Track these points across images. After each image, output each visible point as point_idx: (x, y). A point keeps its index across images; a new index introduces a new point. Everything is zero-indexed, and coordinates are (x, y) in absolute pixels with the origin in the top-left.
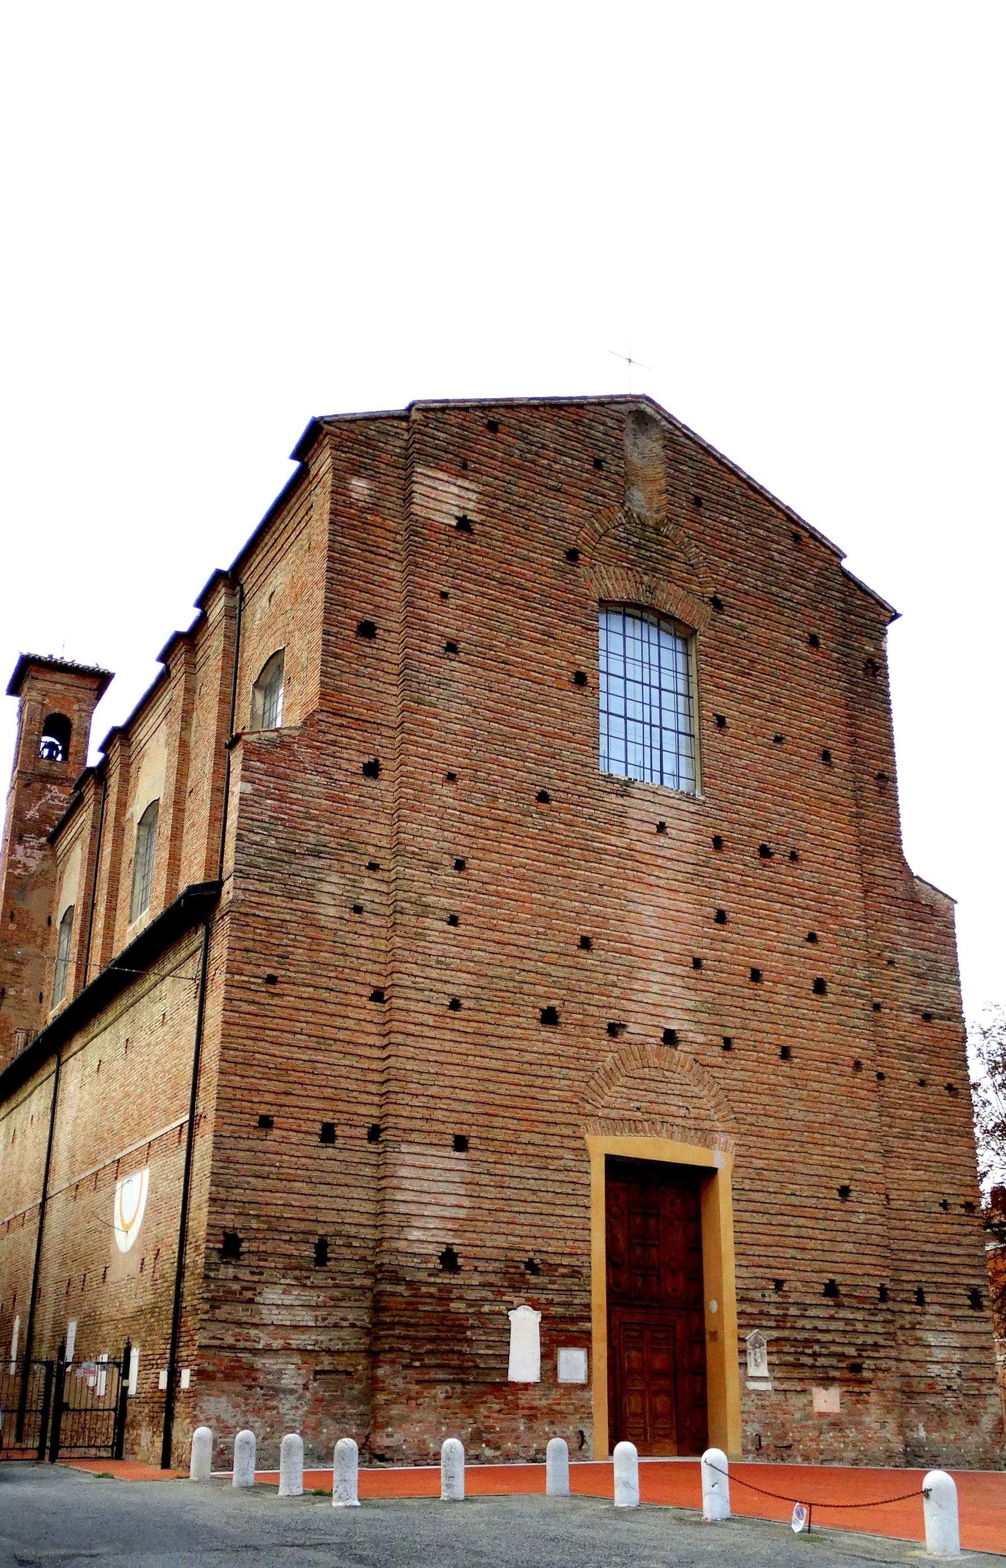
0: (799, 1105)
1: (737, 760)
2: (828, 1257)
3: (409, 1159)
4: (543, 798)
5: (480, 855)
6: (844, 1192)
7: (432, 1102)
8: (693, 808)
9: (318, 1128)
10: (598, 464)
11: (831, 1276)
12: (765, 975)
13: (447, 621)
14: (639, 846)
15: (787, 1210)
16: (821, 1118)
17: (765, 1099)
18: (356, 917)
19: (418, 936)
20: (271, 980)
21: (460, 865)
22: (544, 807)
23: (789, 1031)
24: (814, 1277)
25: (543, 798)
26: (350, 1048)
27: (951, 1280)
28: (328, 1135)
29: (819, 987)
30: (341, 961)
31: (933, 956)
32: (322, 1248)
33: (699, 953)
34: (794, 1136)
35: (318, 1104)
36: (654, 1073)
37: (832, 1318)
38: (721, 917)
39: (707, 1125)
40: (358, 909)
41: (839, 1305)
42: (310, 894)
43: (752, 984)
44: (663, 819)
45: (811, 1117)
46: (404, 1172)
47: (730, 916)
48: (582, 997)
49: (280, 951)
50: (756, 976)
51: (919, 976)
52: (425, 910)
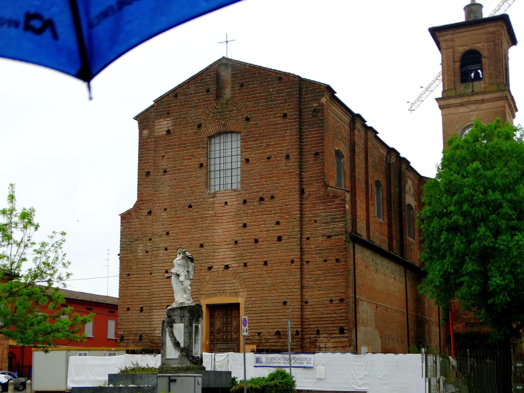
0: (269, 279)
1: (252, 172)
2: (277, 324)
3: (155, 314)
4: (190, 206)
5: (172, 229)
6: (285, 303)
7: (161, 298)
8: (236, 193)
9: (139, 309)
10: (208, 91)
11: (278, 330)
12: (259, 240)
13: (164, 164)
14: (218, 212)
15: (262, 311)
16: (278, 281)
17: (257, 279)
18: (147, 254)
19: (157, 256)
20: (129, 275)
21: (168, 234)
22: (190, 209)
23: (267, 256)
24: (271, 330)
25: (190, 206)
26: (146, 288)
27: (331, 325)
28: (142, 310)
29: (280, 239)
30: (143, 266)
31: (334, 214)
32: (141, 336)
33: (236, 239)
34: (266, 289)
35: (139, 303)
36: (221, 278)
37: (277, 342)
38: (245, 226)
39: (237, 291)
40: (147, 252)
41: (281, 338)
42: (136, 251)
43: (254, 244)
44: (226, 201)
45: (274, 281)
46: (154, 317)
47: (248, 224)
48: (200, 262)
49: (129, 267)
50: (256, 241)
51: (326, 223)
52: (158, 248)
